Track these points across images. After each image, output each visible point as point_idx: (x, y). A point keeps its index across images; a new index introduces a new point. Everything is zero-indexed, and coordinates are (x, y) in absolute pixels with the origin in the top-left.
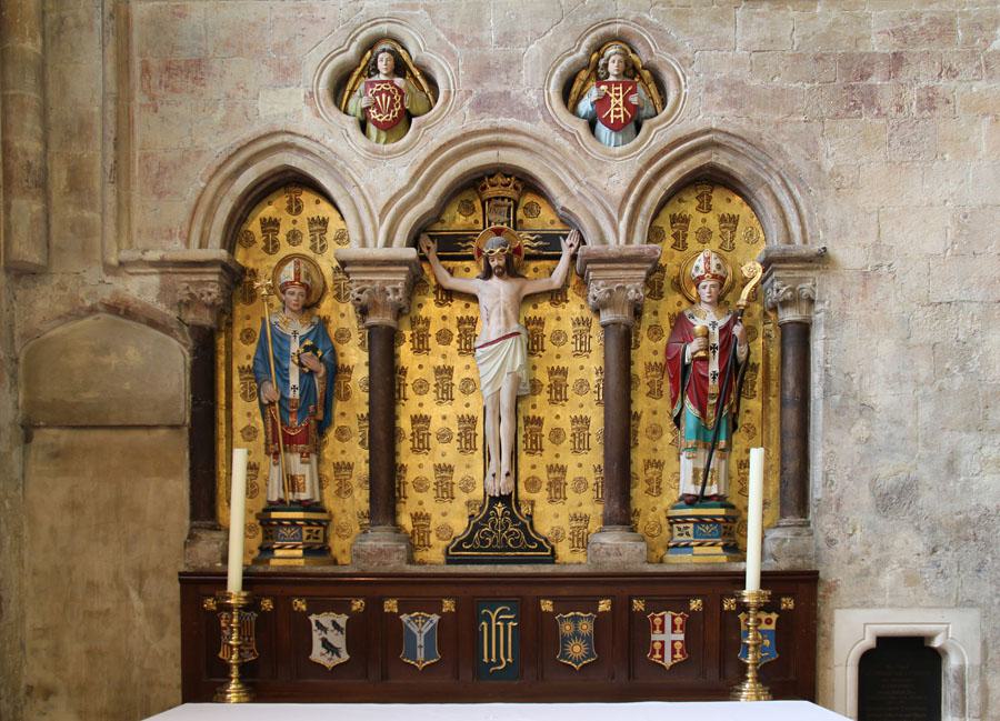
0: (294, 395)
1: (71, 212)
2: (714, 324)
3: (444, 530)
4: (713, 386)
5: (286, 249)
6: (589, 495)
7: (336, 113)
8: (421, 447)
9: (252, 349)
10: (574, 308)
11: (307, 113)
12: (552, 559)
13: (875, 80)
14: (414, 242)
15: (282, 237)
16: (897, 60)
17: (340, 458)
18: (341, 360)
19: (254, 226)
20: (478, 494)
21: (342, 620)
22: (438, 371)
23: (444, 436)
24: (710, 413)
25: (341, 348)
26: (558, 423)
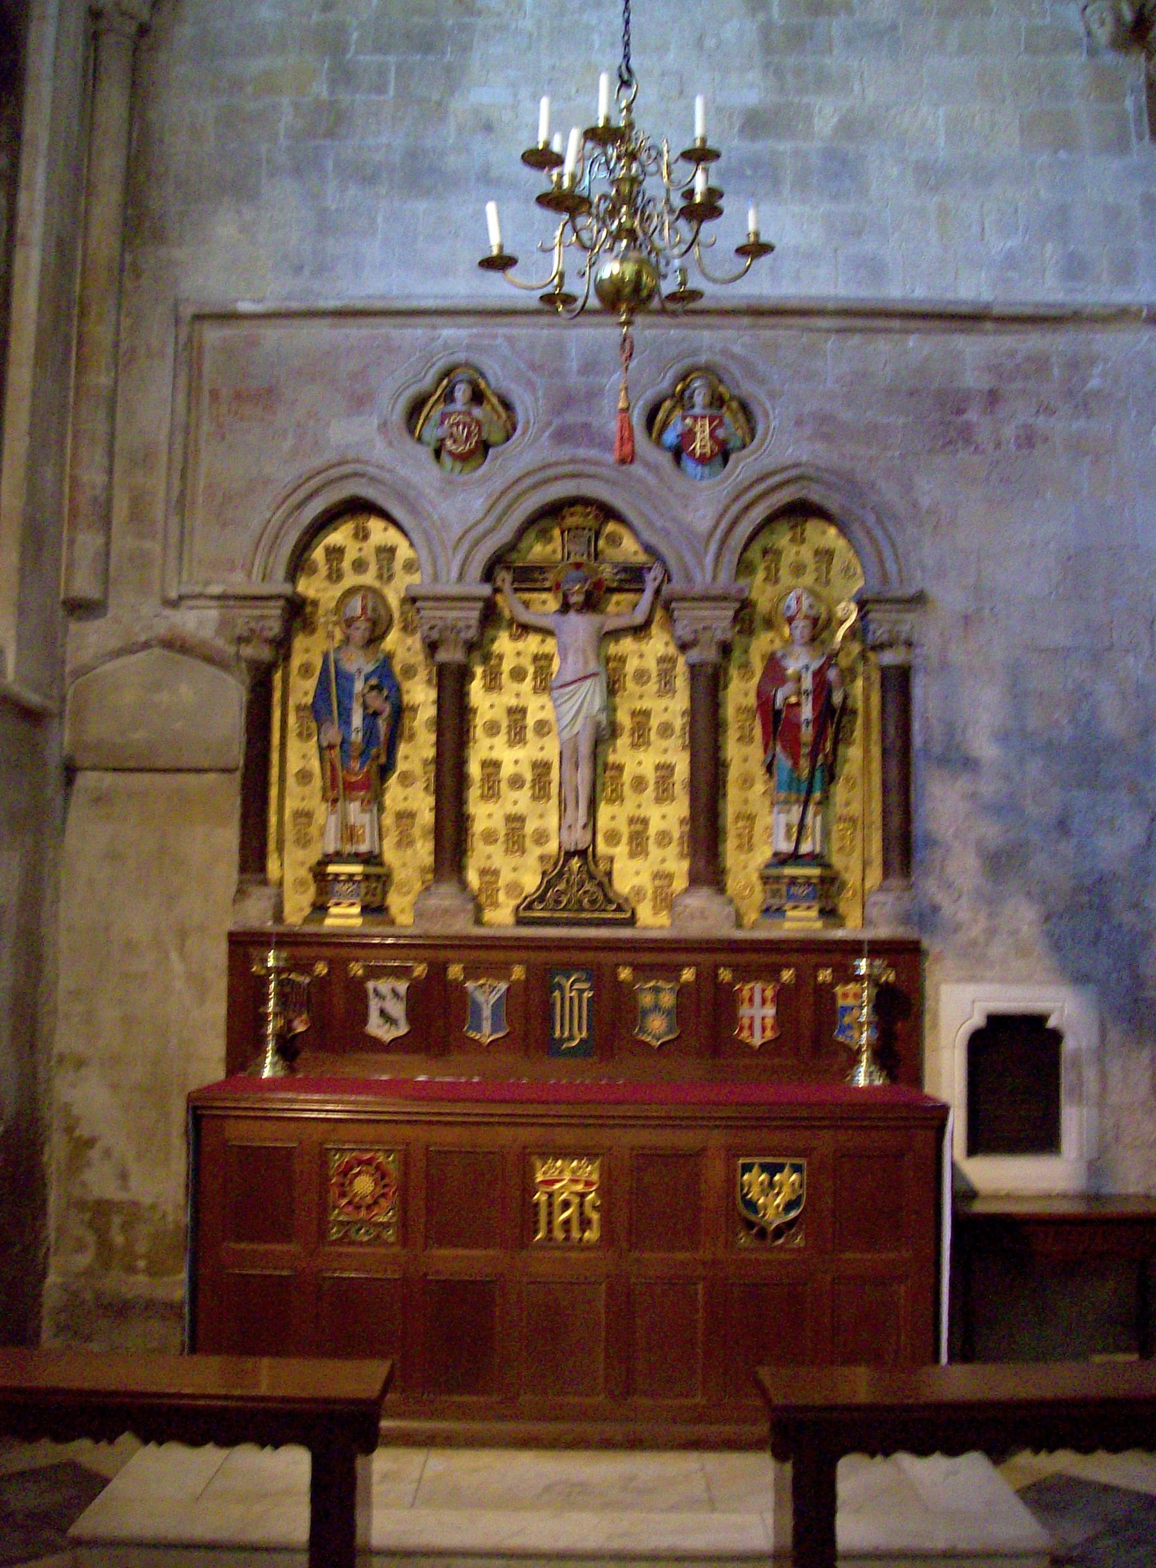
0: (357, 737)
1: (131, 542)
2: (807, 667)
3: (514, 888)
4: (807, 734)
5: (351, 580)
6: (673, 849)
7: (410, 444)
8: (491, 792)
9: (311, 684)
10: (658, 644)
11: (380, 444)
12: (632, 921)
13: (972, 415)
14: (488, 576)
15: (346, 564)
16: (993, 398)
17: (401, 806)
18: (406, 699)
19: (318, 554)
20: (552, 847)
21: (402, 987)
22: (511, 711)
23: (516, 782)
24: (804, 763)
25: (406, 685)
26: (640, 770)
